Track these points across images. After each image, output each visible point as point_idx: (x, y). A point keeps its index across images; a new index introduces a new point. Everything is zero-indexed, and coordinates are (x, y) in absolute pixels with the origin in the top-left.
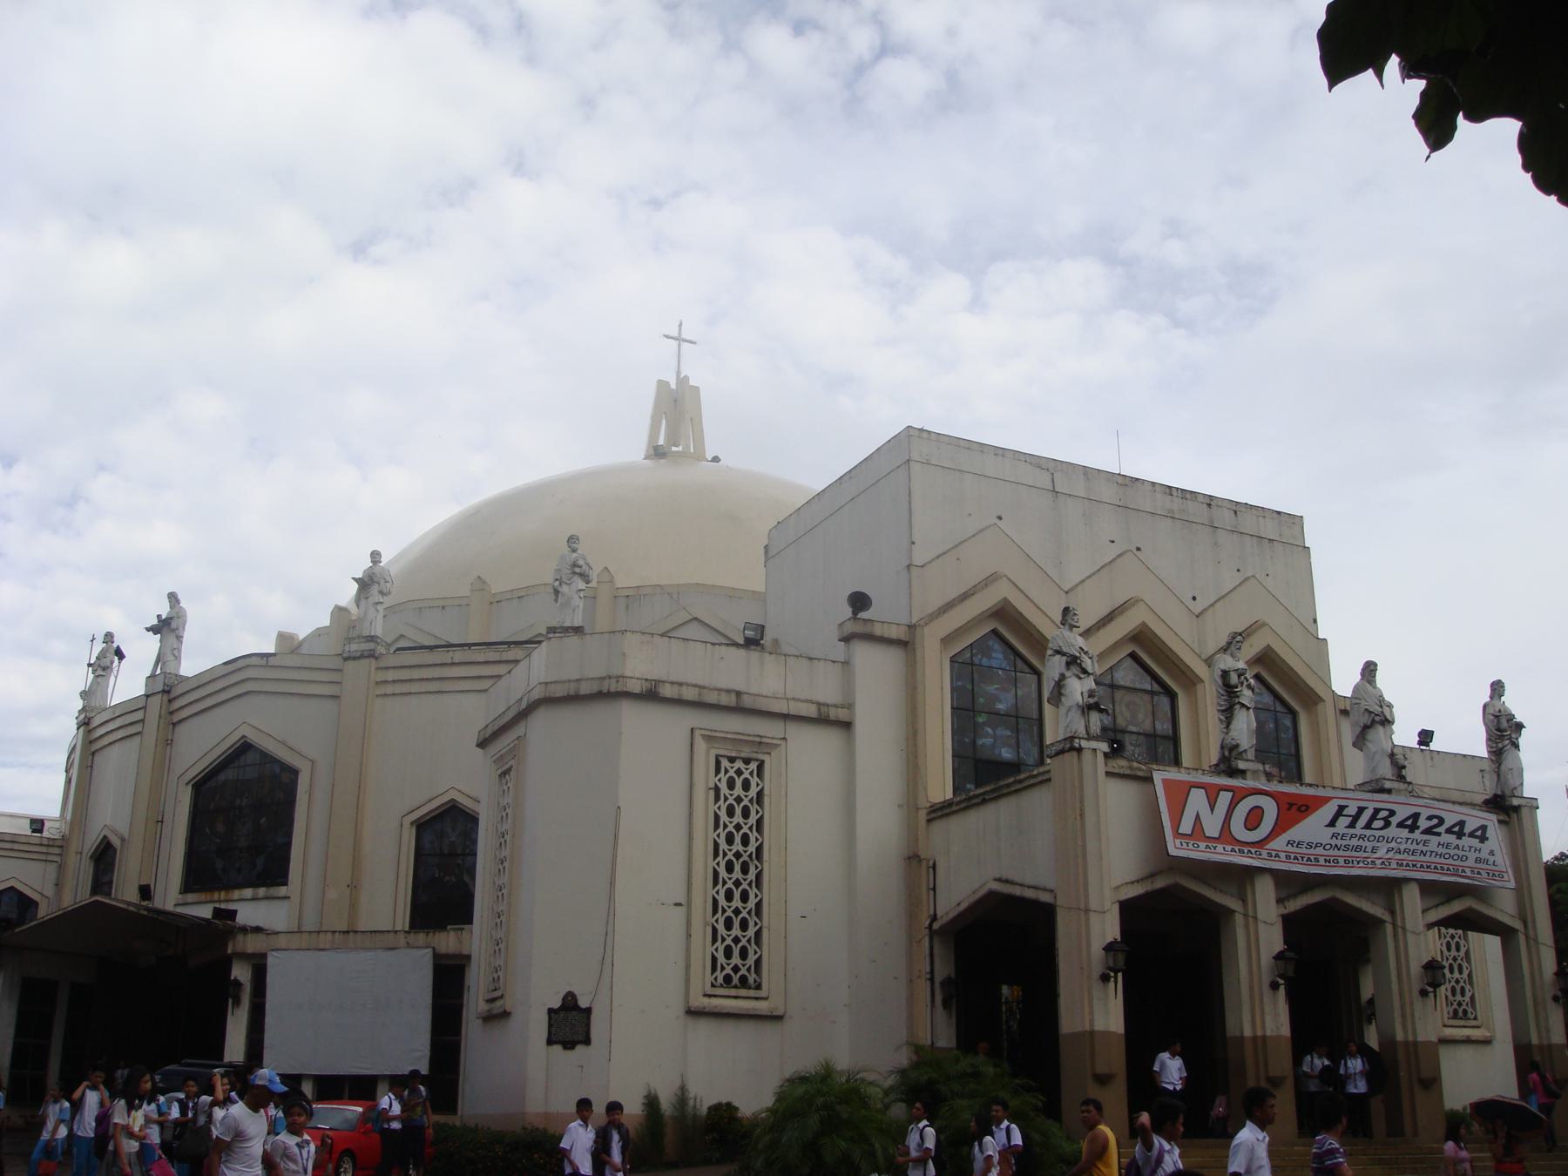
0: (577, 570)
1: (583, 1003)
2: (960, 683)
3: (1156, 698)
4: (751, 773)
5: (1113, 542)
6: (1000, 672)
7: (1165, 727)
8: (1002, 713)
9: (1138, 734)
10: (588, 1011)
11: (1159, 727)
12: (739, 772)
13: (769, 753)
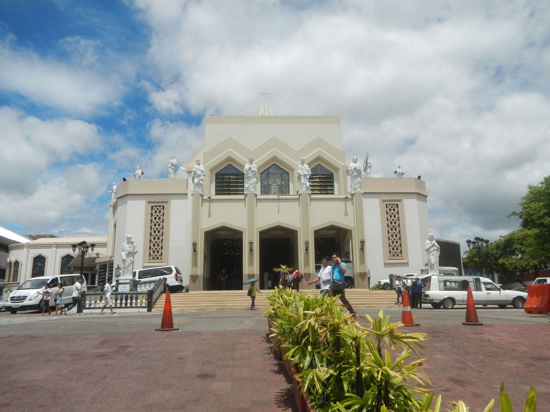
1: (120, 267)
3: (283, 175)
4: (161, 209)
7: (285, 182)
9: (276, 186)
11: (283, 183)
12: (158, 209)
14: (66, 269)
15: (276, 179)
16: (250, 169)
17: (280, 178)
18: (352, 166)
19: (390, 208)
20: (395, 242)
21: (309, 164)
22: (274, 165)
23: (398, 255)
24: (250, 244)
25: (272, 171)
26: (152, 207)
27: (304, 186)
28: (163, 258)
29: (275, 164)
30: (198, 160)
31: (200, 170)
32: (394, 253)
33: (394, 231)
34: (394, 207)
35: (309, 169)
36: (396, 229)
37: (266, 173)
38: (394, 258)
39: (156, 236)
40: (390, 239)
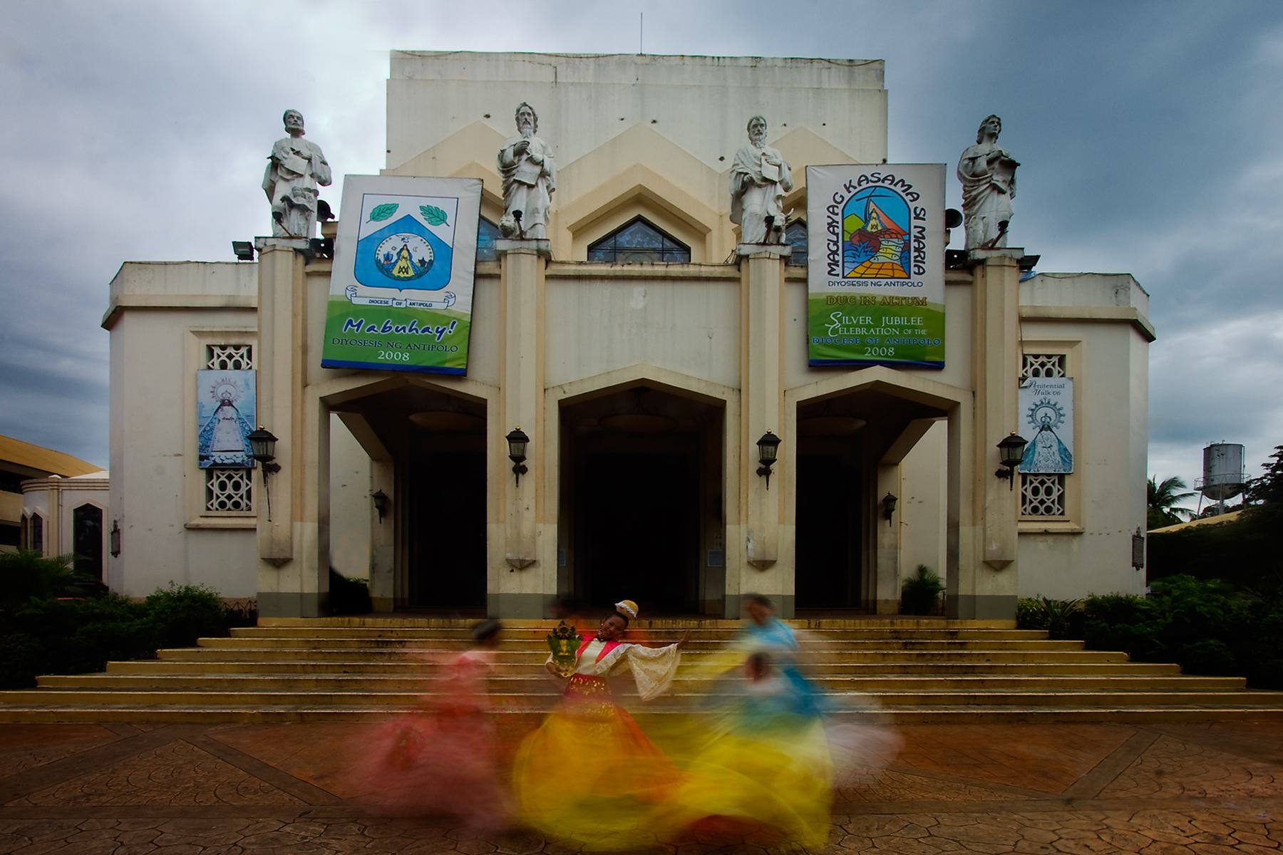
5: (622, 119)
22: (638, 226)
23: (1048, 510)
25: (628, 242)
29: (639, 219)
32: (1036, 503)
38: (1035, 517)
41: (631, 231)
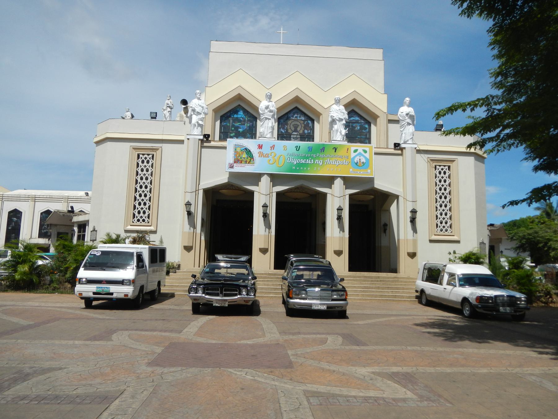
0: (168, 105)
2: (225, 124)
4: (150, 158)
6: (241, 119)
7: (309, 131)
8: (241, 132)
9: (297, 135)
10: (96, 231)
13: (156, 152)
14: (45, 226)
15: (297, 127)
16: (267, 108)
17: (303, 125)
18: (403, 110)
19: (440, 170)
20: (444, 213)
21: (346, 106)
23: (446, 231)
24: (264, 208)
26: (138, 155)
27: (339, 133)
28: (150, 221)
29: (296, 108)
30: (198, 93)
31: (200, 106)
33: (443, 199)
34: (445, 170)
35: (346, 112)
36: (445, 198)
37: (285, 118)
38: (442, 233)
39: (142, 192)
40: (438, 210)
41: (293, 112)
